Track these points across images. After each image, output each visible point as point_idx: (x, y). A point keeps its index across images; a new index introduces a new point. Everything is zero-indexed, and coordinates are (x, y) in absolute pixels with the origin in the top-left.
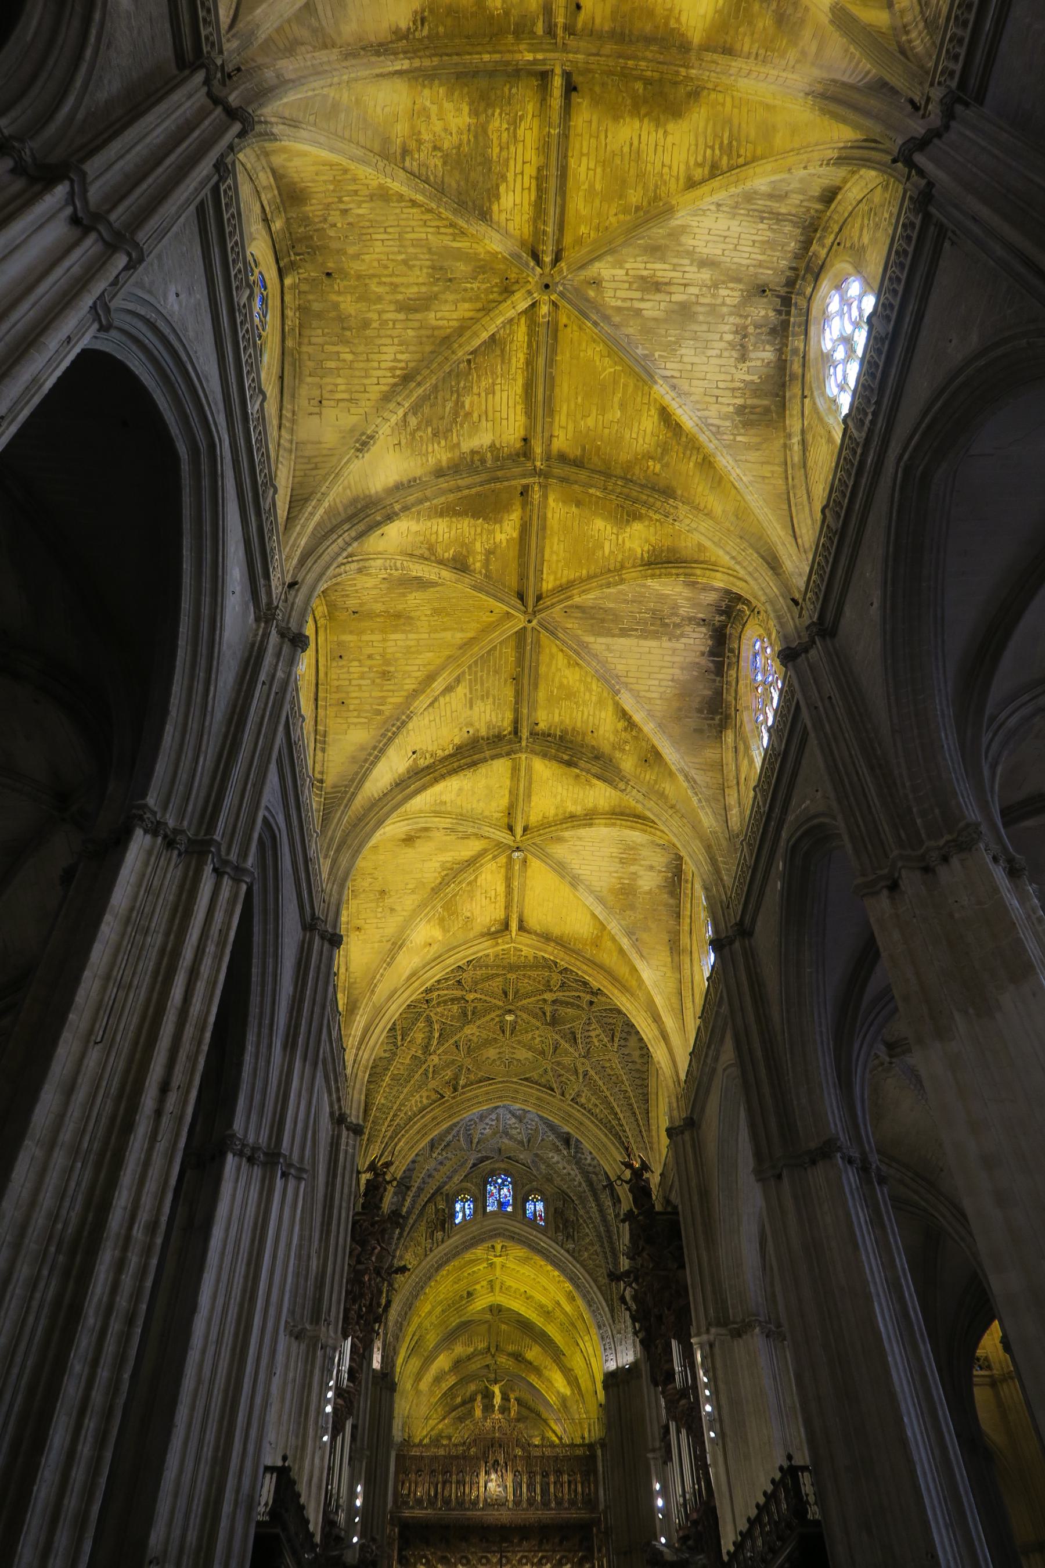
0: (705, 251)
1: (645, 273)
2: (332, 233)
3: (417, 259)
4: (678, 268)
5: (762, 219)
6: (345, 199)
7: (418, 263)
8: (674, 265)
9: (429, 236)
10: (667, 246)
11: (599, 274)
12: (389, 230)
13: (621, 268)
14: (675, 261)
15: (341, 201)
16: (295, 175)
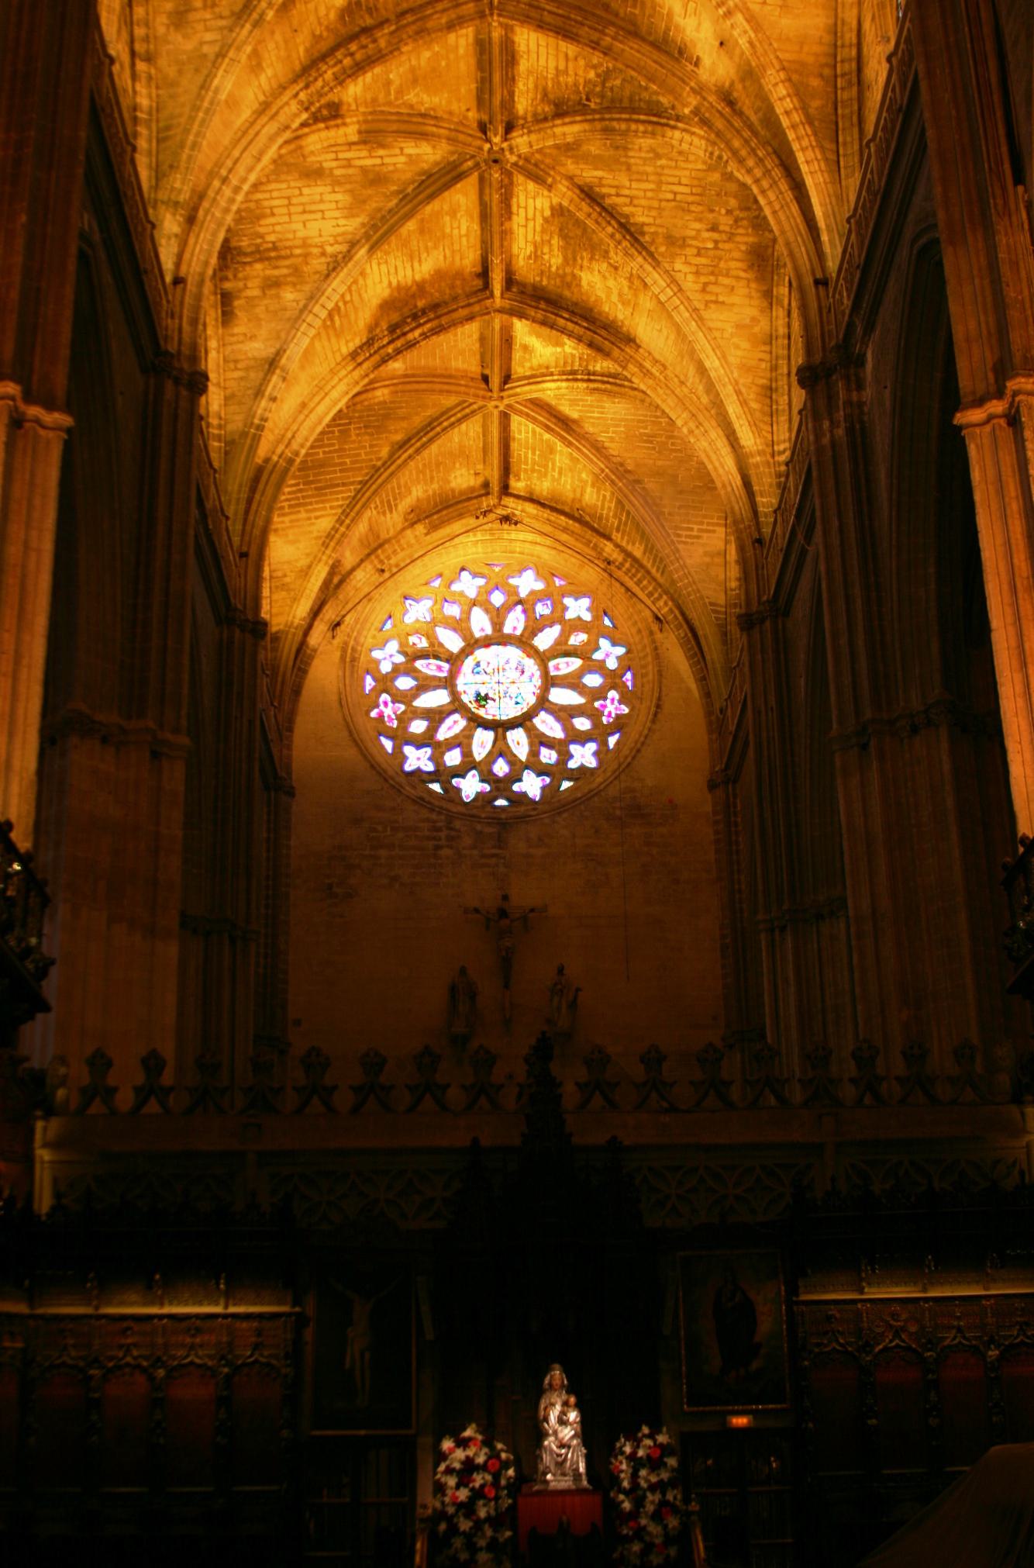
0: (320, 189)
1: (381, 152)
2: (733, 203)
3: (645, 159)
4: (345, 163)
5: (275, 248)
6: (710, 245)
7: (643, 155)
8: (350, 166)
9: (627, 184)
10: (364, 187)
11: (434, 147)
12: (670, 196)
13: (410, 156)
14: (351, 171)
15: (716, 242)
16: (754, 294)
